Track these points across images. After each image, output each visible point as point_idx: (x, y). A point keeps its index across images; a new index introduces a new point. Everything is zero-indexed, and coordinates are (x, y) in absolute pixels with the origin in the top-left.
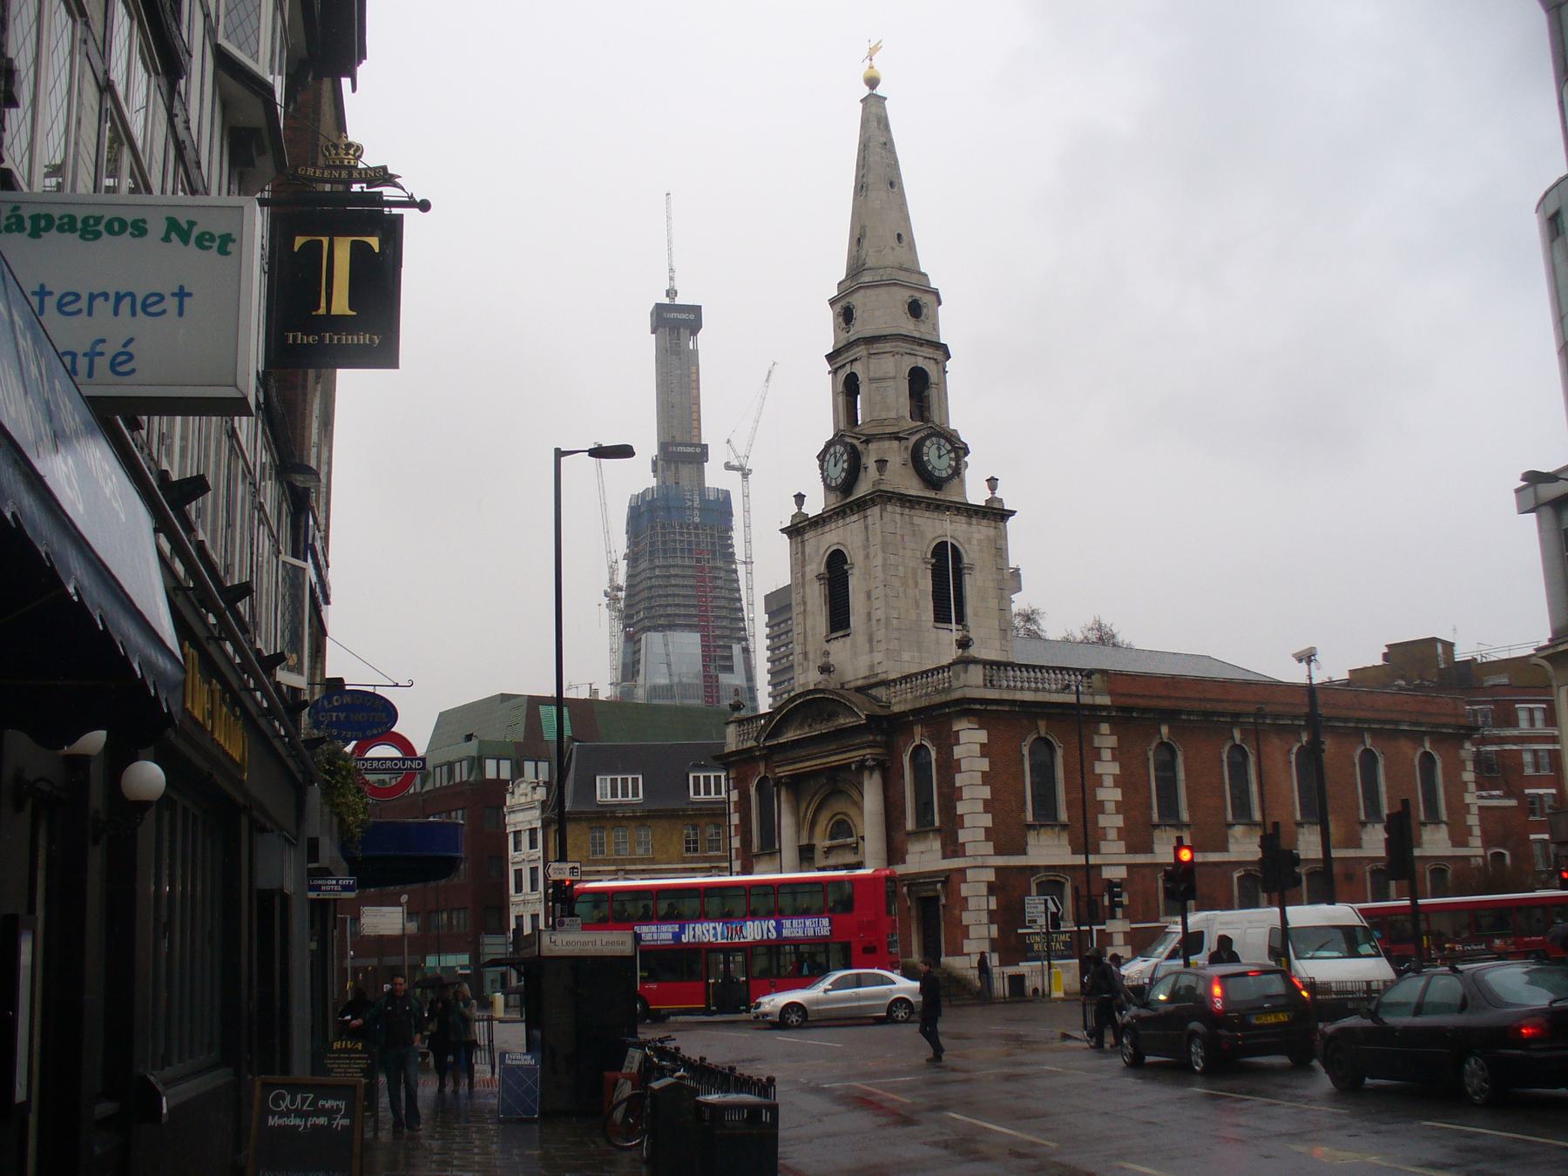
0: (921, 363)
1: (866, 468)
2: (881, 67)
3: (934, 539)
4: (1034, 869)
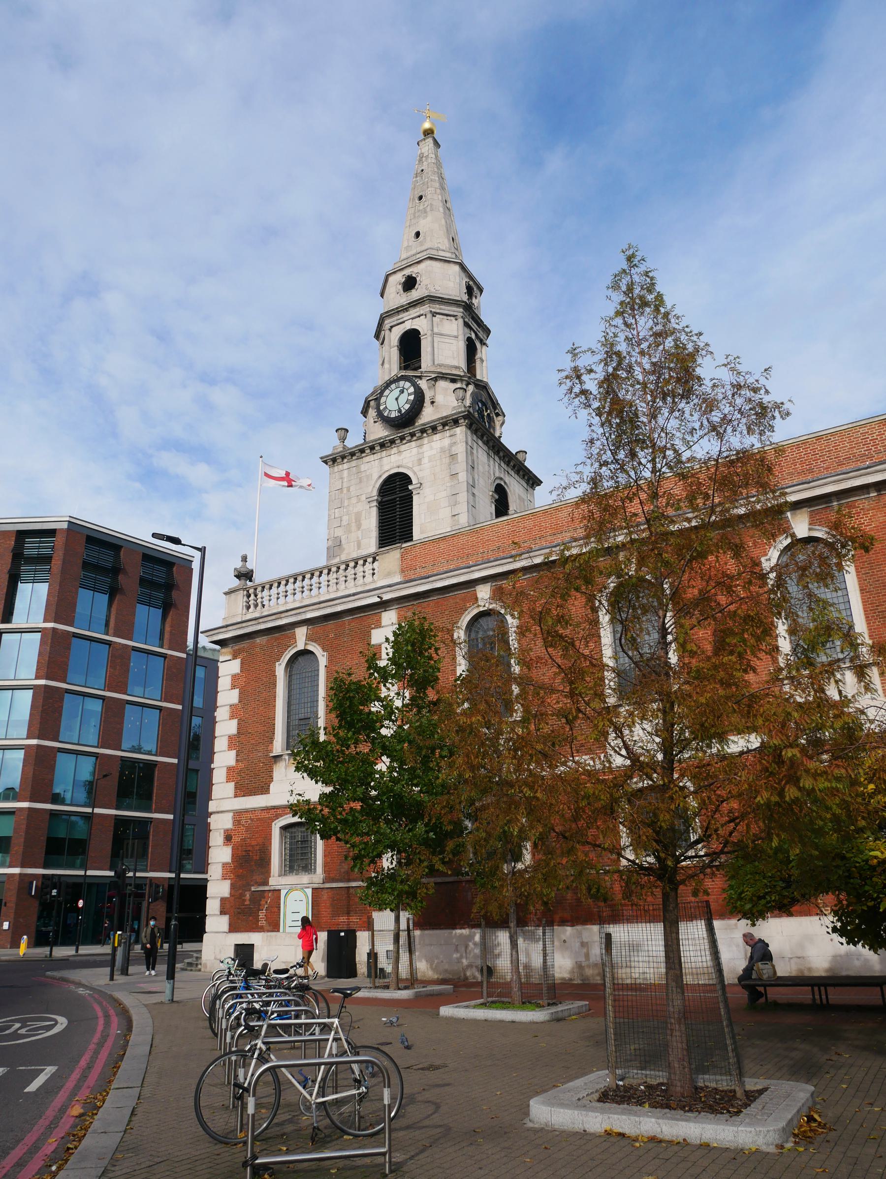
0: (408, 326)
3: (380, 476)
4: (276, 811)
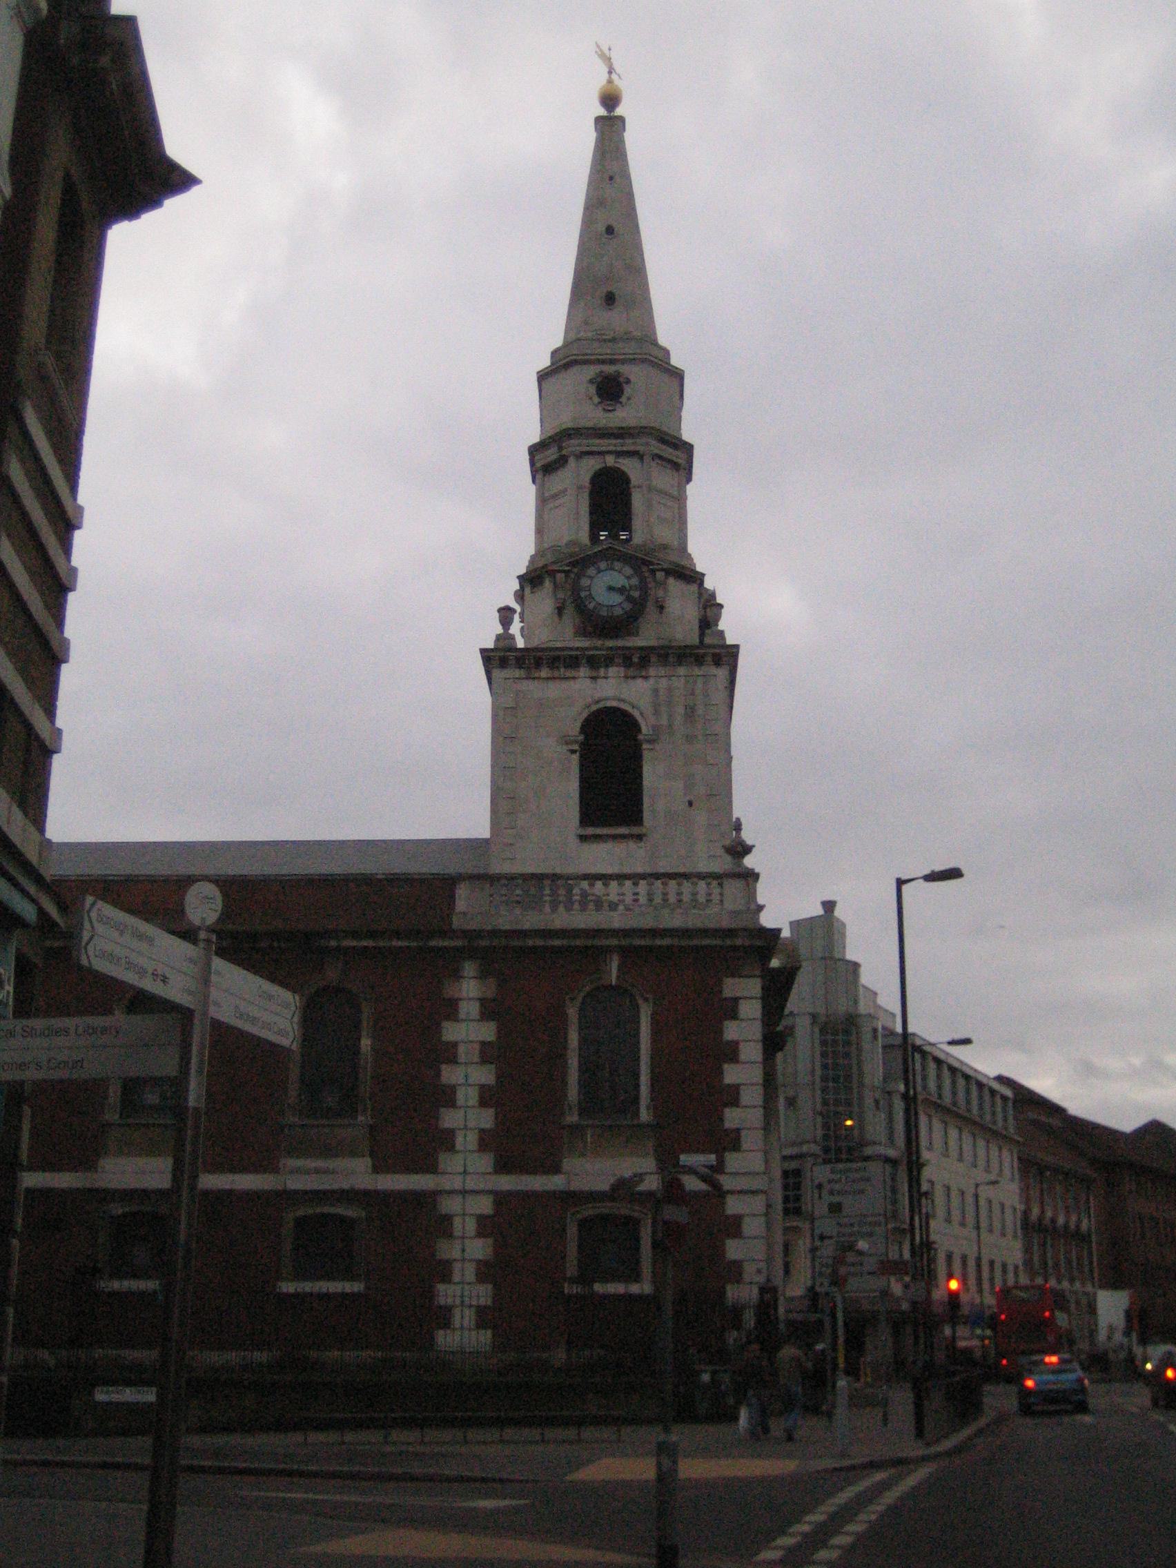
1: (661, 608)
2: (624, 85)
